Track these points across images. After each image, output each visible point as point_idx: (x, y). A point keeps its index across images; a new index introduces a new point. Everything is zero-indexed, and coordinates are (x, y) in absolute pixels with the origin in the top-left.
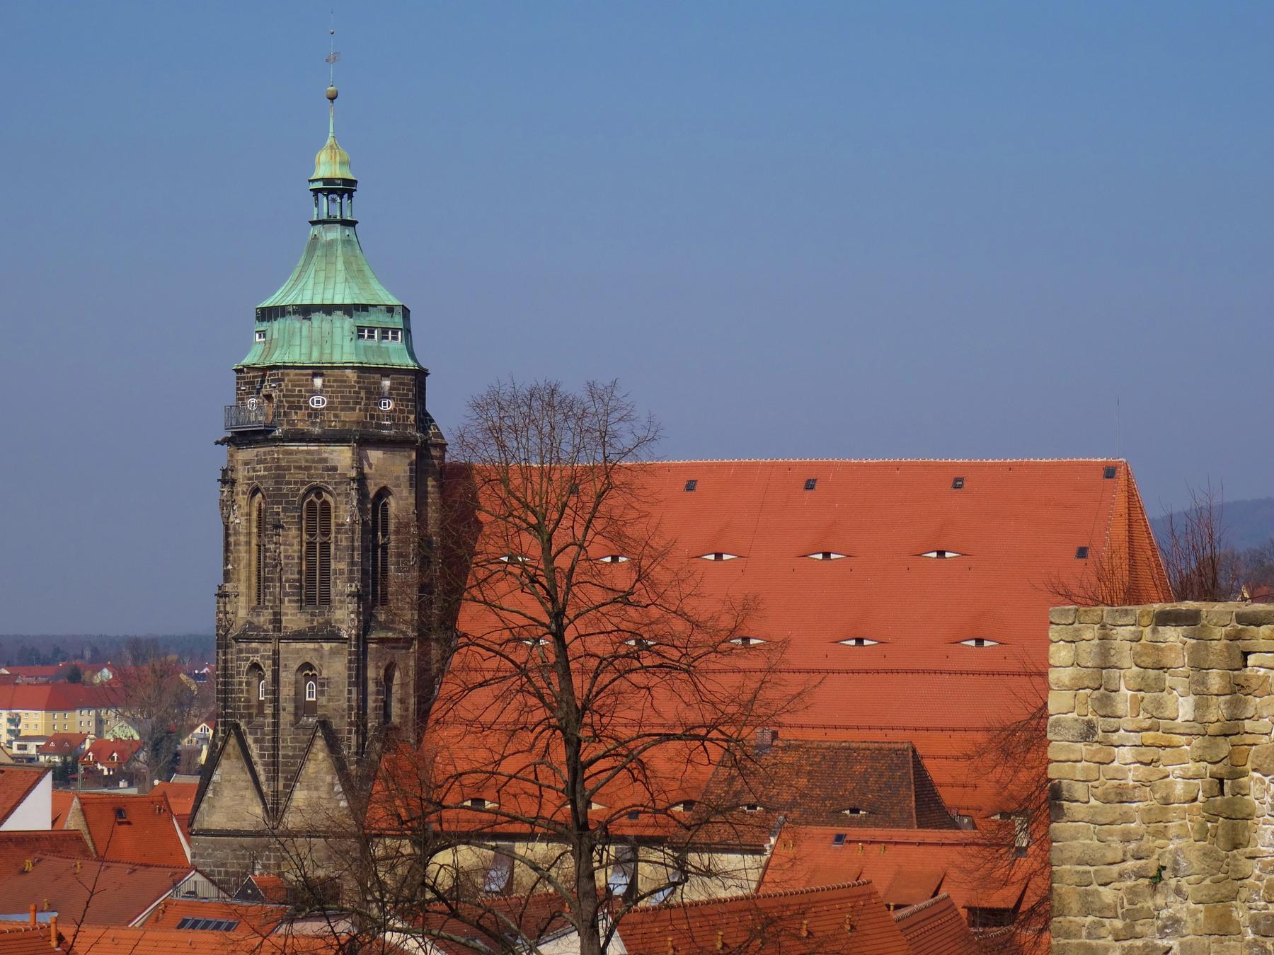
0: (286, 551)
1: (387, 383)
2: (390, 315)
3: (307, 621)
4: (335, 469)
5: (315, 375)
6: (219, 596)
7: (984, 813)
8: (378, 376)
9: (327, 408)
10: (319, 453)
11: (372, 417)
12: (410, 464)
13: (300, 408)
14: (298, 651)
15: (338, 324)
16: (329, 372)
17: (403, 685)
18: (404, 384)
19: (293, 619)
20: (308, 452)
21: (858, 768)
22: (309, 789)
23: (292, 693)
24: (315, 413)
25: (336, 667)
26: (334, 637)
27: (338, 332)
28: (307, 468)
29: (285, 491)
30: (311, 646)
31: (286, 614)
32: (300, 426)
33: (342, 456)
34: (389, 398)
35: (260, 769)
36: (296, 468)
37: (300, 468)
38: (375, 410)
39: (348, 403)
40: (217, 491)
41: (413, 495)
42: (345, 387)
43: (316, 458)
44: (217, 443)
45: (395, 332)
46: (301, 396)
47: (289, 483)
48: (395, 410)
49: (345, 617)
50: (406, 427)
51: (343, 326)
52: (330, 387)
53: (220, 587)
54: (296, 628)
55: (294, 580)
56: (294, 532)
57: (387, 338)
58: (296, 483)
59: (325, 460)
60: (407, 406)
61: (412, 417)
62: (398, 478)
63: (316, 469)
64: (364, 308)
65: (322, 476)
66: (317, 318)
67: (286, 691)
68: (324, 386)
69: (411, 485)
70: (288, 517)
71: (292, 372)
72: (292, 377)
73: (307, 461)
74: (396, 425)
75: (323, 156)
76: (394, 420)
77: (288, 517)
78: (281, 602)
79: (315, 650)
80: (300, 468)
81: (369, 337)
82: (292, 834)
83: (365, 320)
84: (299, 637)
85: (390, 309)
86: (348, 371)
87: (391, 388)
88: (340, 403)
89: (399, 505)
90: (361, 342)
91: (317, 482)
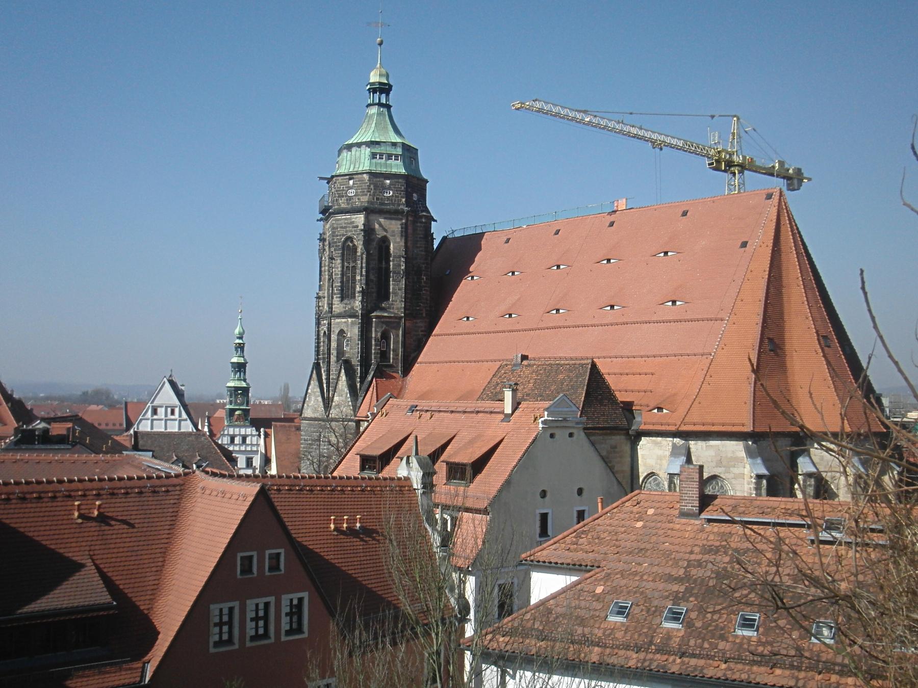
0: (335, 271)
1: (388, 182)
2: (394, 147)
3: (343, 307)
4: (357, 227)
5: (350, 179)
6: (317, 298)
7: (649, 408)
8: (382, 179)
9: (355, 196)
10: (350, 219)
11: (378, 199)
12: (402, 224)
13: (343, 197)
14: (338, 323)
15: (363, 152)
16: (356, 176)
17: (396, 342)
18: (399, 182)
19: (338, 307)
20: (346, 219)
21: (561, 377)
22: (339, 396)
23: (336, 346)
24: (350, 198)
25: (353, 331)
26: (353, 315)
27: (363, 156)
28: (345, 227)
29: (335, 240)
30: (344, 320)
31: (335, 304)
32: (343, 206)
33: (360, 219)
34: (390, 190)
35: (325, 386)
36: (340, 227)
37: (342, 227)
38: (380, 195)
39: (364, 192)
40: (317, 244)
41: (403, 241)
42: (363, 183)
43: (349, 221)
44: (318, 220)
45: (397, 156)
46: (343, 190)
47: (337, 236)
48: (392, 196)
49: (357, 304)
50: (399, 205)
51: (367, 151)
52: (357, 184)
53: (317, 294)
54: (338, 311)
55: (339, 286)
56: (339, 261)
57: (392, 159)
58: (340, 235)
59: (353, 222)
60: (400, 194)
61: (404, 200)
62: (393, 231)
63: (349, 227)
64: (378, 143)
65: (351, 231)
66: (354, 149)
67: (334, 345)
68: (354, 184)
69: (402, 236)
70: (336, 253)
71: (340, 178)
72: (340, 181)
73: (345, 224)
74: (393, 204)
75: (372, 74)
76: (392, 201)
77: (336, 253)
78: (332, 298)
79: (345, 322)
80: (342, 227)
81: (380, 158)
82: (333, 420)
83: (377, 150)
84: (339, 316)
85: (394, 144)
86: (365, 175)
87: (391, 184)
88: (361, 192)
89: (396, 246)
90: (374, 161)
91: (349, 234)
